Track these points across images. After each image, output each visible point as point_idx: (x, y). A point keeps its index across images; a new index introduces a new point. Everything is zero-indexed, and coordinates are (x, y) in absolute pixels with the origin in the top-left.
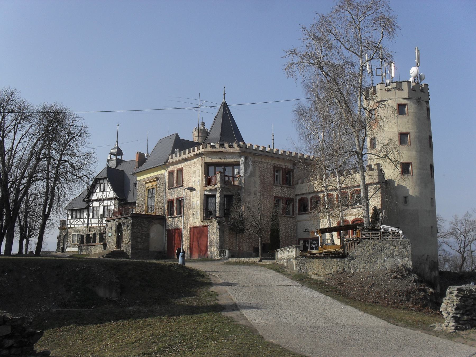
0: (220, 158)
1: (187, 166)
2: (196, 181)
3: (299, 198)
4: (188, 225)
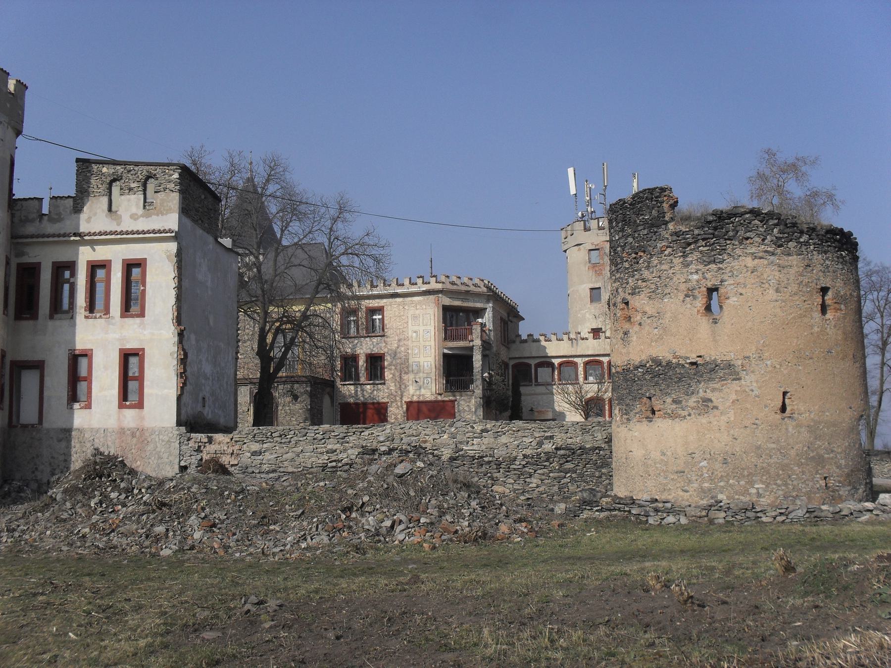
0: (462, 300)
1: (395, 306)
2: (421, 331)
3: (512, 363)
4: (401, 398)
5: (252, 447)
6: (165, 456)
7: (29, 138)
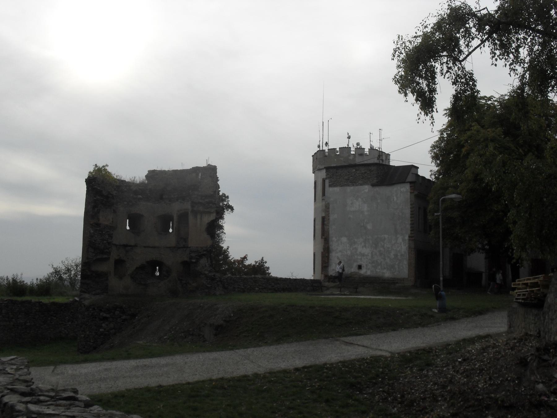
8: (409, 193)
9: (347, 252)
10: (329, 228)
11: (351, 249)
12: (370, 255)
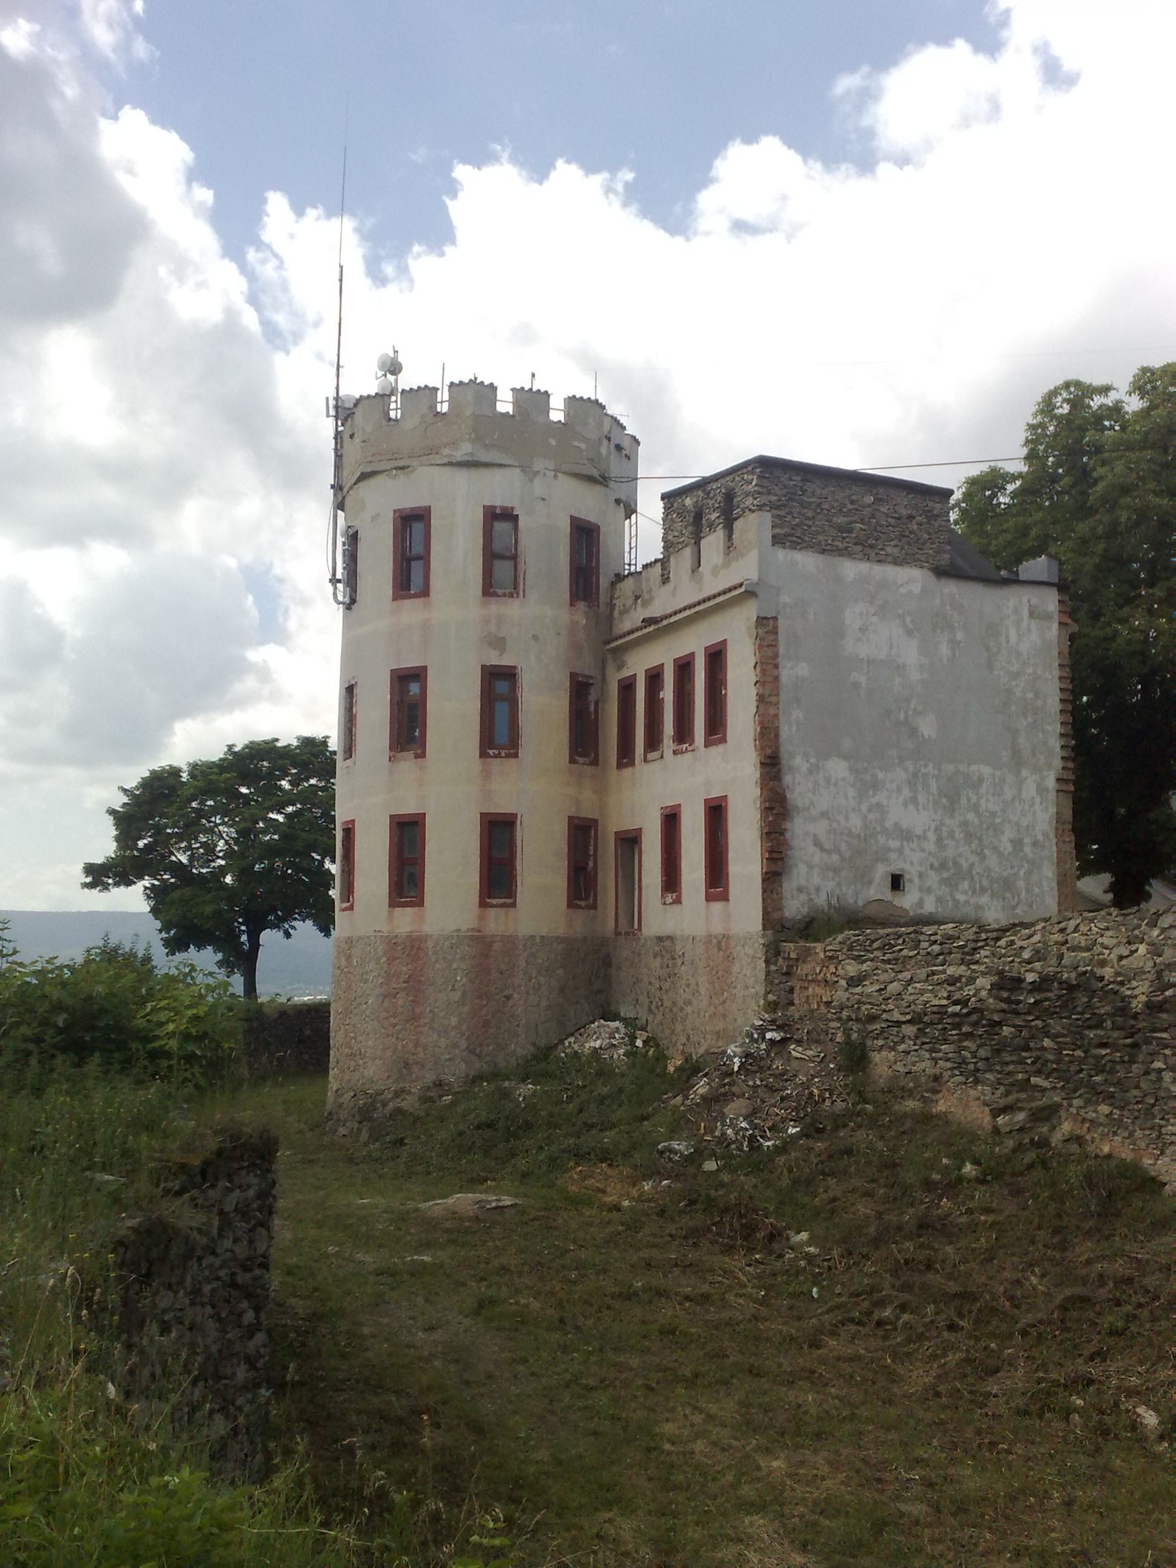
5: (849, 968)
6: (751, 982)
7: (624, 480)
8: (1055, 625)
9: (847, 819)
10: (776, 716)
11: (864, 808)
12: (932, 836)
